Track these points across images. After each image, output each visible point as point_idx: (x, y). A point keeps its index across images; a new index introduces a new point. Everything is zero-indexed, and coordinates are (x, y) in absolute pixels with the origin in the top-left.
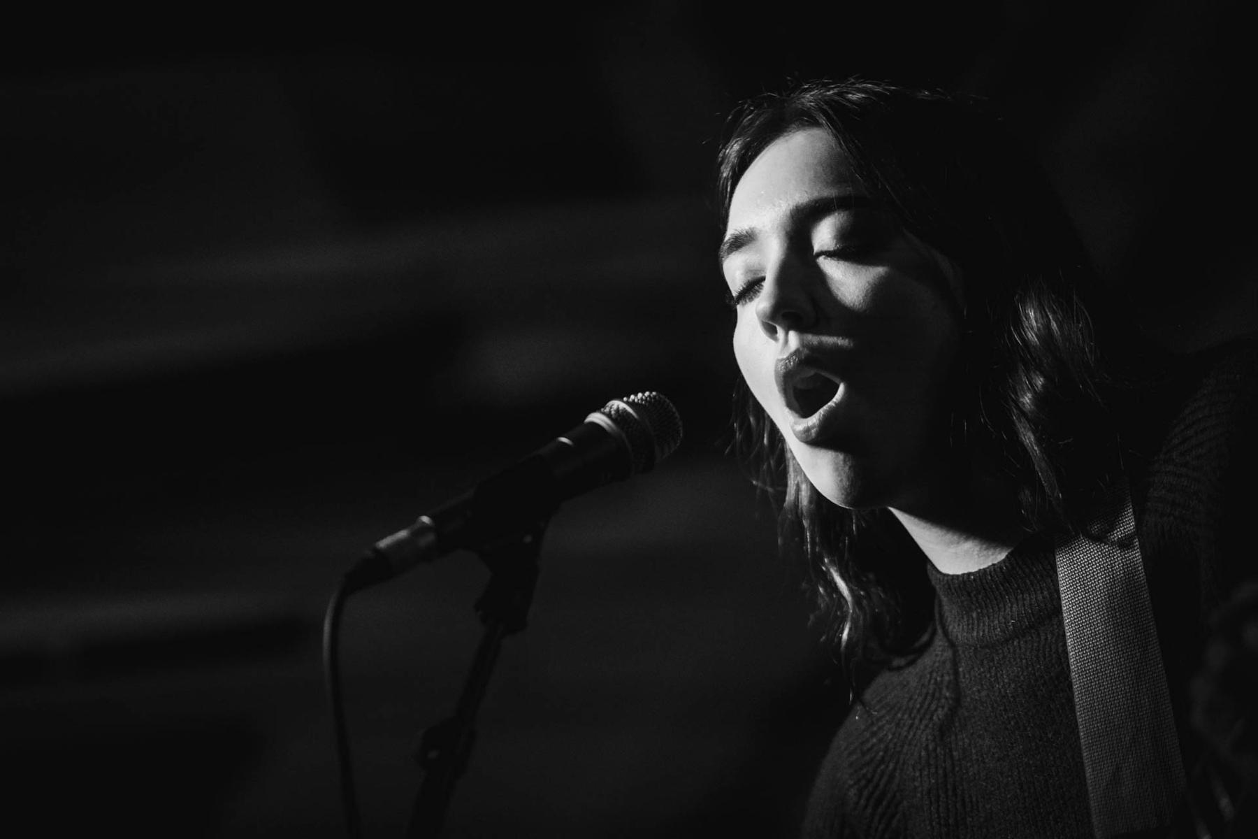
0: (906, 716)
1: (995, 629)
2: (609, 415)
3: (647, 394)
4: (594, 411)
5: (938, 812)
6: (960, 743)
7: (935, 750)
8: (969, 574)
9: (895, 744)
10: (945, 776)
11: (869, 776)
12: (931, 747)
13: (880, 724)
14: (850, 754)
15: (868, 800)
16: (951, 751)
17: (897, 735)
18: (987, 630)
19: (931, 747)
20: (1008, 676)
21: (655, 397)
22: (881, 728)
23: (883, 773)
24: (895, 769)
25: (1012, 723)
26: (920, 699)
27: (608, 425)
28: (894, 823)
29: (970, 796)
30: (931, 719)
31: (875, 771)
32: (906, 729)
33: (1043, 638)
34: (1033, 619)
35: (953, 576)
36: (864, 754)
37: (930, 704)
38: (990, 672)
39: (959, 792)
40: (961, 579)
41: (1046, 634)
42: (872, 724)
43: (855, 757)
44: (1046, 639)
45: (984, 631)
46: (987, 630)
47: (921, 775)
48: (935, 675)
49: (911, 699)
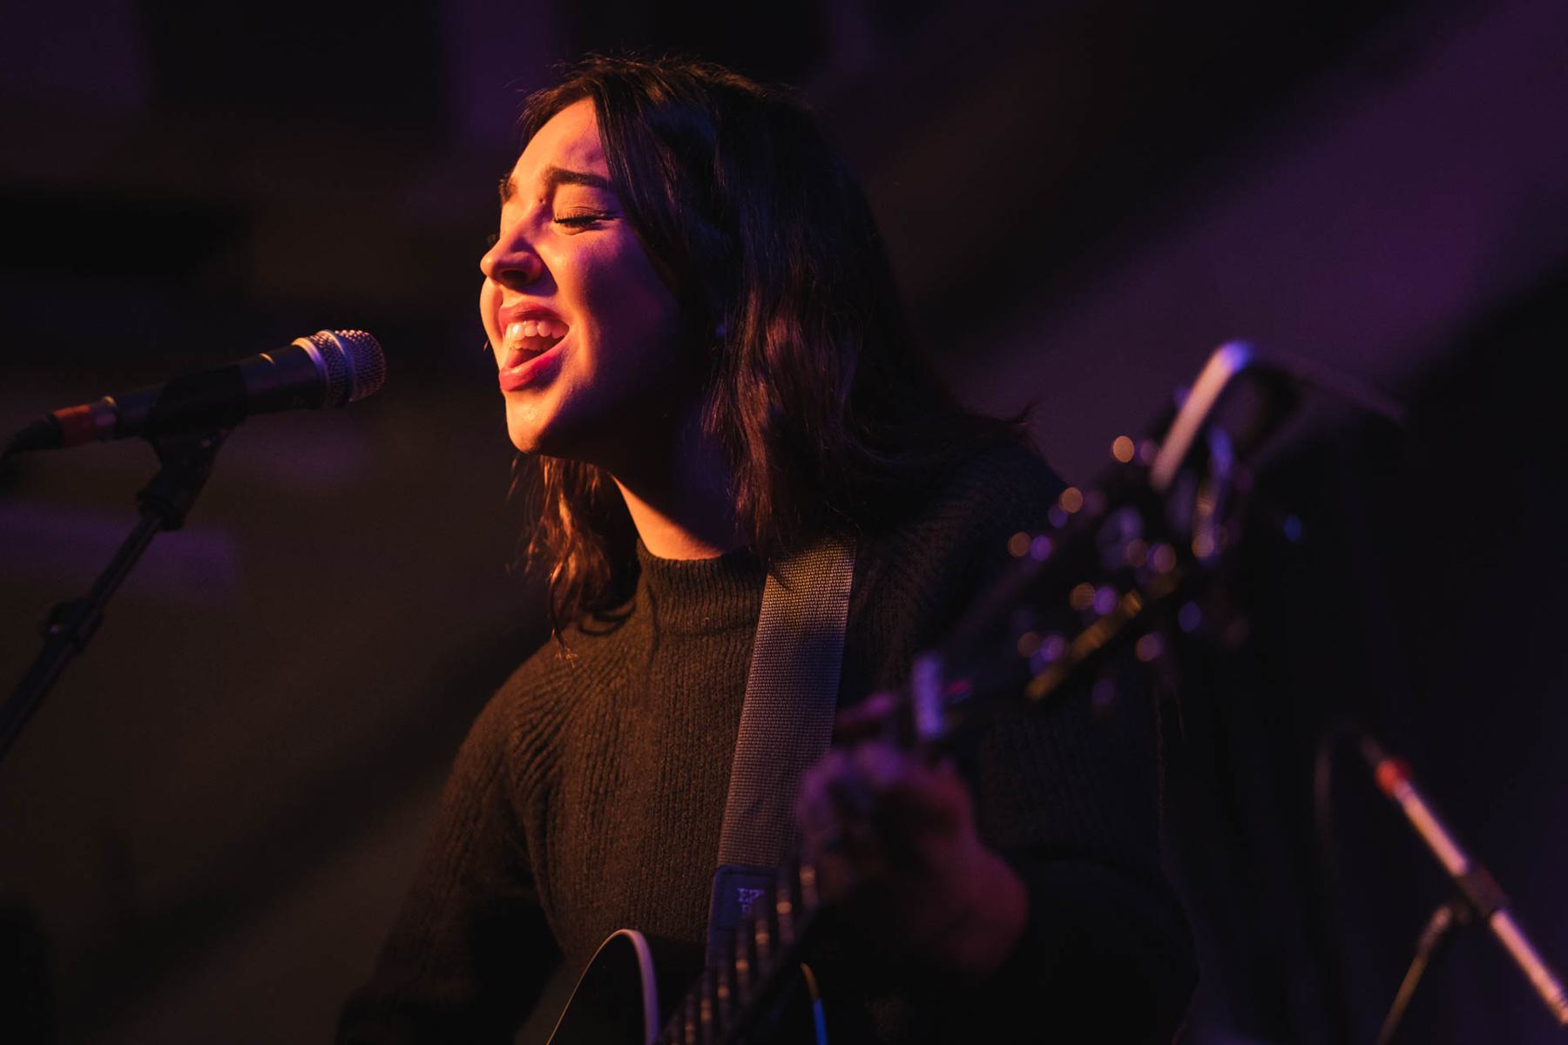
0: (585, 675)
1: (688, 619)
2: (316, 344)
3: (360, 332)
4: (304, 336)
6: (629, 717)
7: (604, 716)
10: (607, 745)
11: (535, 722)
12: (602, 712)
13: (559, 673)
14: (523, 695)
15: (529, 745)
16: (619, 721)
17: (572, 690)
18: (679, 617)
21: (366, 336)
22: (558, 678)
24: (562, 723)
26: (604, 663)
27: (315, 355)
28: (551, 773)
29: (624, 771)
30: (608, 685)
31: (542, 718)
32: (583, 687)
36: (535, 699)
37: (611, 670)
38: (672, 658)
39: (615, 764)
42: (551, 672)
43: (526, 699)
45: (676, 618)
46: (679, 617)
47: (585, 736)
48: (623, 644)
49: (595, 659)
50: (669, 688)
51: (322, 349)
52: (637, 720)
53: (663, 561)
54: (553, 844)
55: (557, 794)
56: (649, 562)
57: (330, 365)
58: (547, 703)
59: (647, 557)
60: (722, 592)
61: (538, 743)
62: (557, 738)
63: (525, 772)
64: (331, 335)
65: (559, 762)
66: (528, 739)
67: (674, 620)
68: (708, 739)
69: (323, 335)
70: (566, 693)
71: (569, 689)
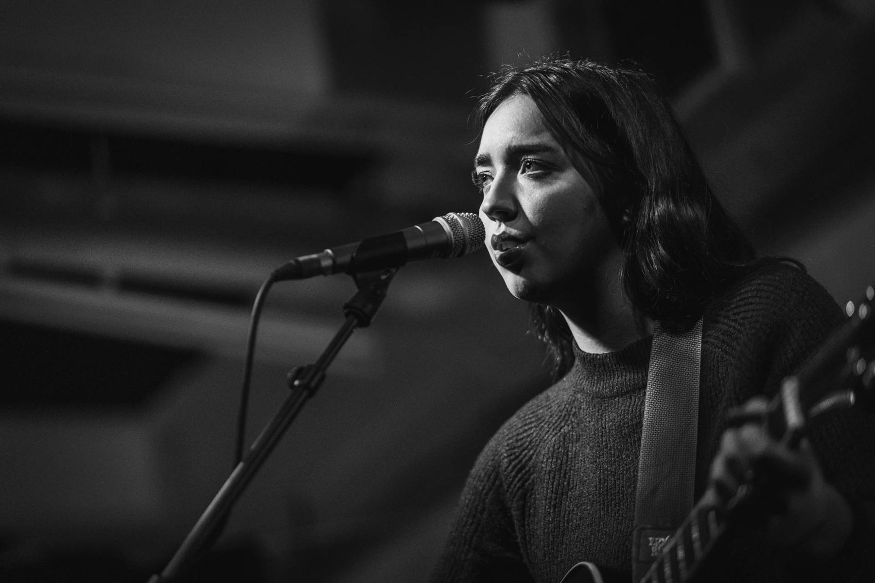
0: (546, 426)
2: (447, 221)
3: (471, 214)
4: (439, 216)
5: (553, 484)
6: (574, 449)
8: (597, 355)
9: (537, 440)
10: (561, 465)
11: (517, 454)
14: (510, 439)
15: (514, 468)
16: (568, 451)
17: (539, 435)
18: (601, 388)
19: (556, 447)
20: (609, 417)
21: (475, 216)
23: (526, 455)
24: (533, 454)
25: (604, 443)
26: (556, 418)
28: (527, 484)
29: (573, 480)
30: (560, 431)
32: (544, 433)
33: (633, 400)
34: (629, 388)
35: (588, 353)
37: (561, 422)
39: (567, 476)
40: (591, 356)
41: (635, 398)
43: (511, 441)
44: (635, 402)
45: (599, 388)
47: (547, 461)
48: (567, 406)
49: (551, 416)
50: (598, 429)
51: (450, 223)
52: (579, 451)
53: (590, 354)
54: (529, 525)
55: (531, 496)
56: (582, 356)
57: (454, 233)
58: (525, 443)
59: (581, 353)
60: (624, 371)
61: (519, 466)
62: (530, 463)
63: (511, 483)
64: (454, 215)
65: (532, 477)
66: (513, 463)
67: (598, 389)
68: (624, 456)
69: (451, 215)
70: (535, 437)
71: (537, 434)
